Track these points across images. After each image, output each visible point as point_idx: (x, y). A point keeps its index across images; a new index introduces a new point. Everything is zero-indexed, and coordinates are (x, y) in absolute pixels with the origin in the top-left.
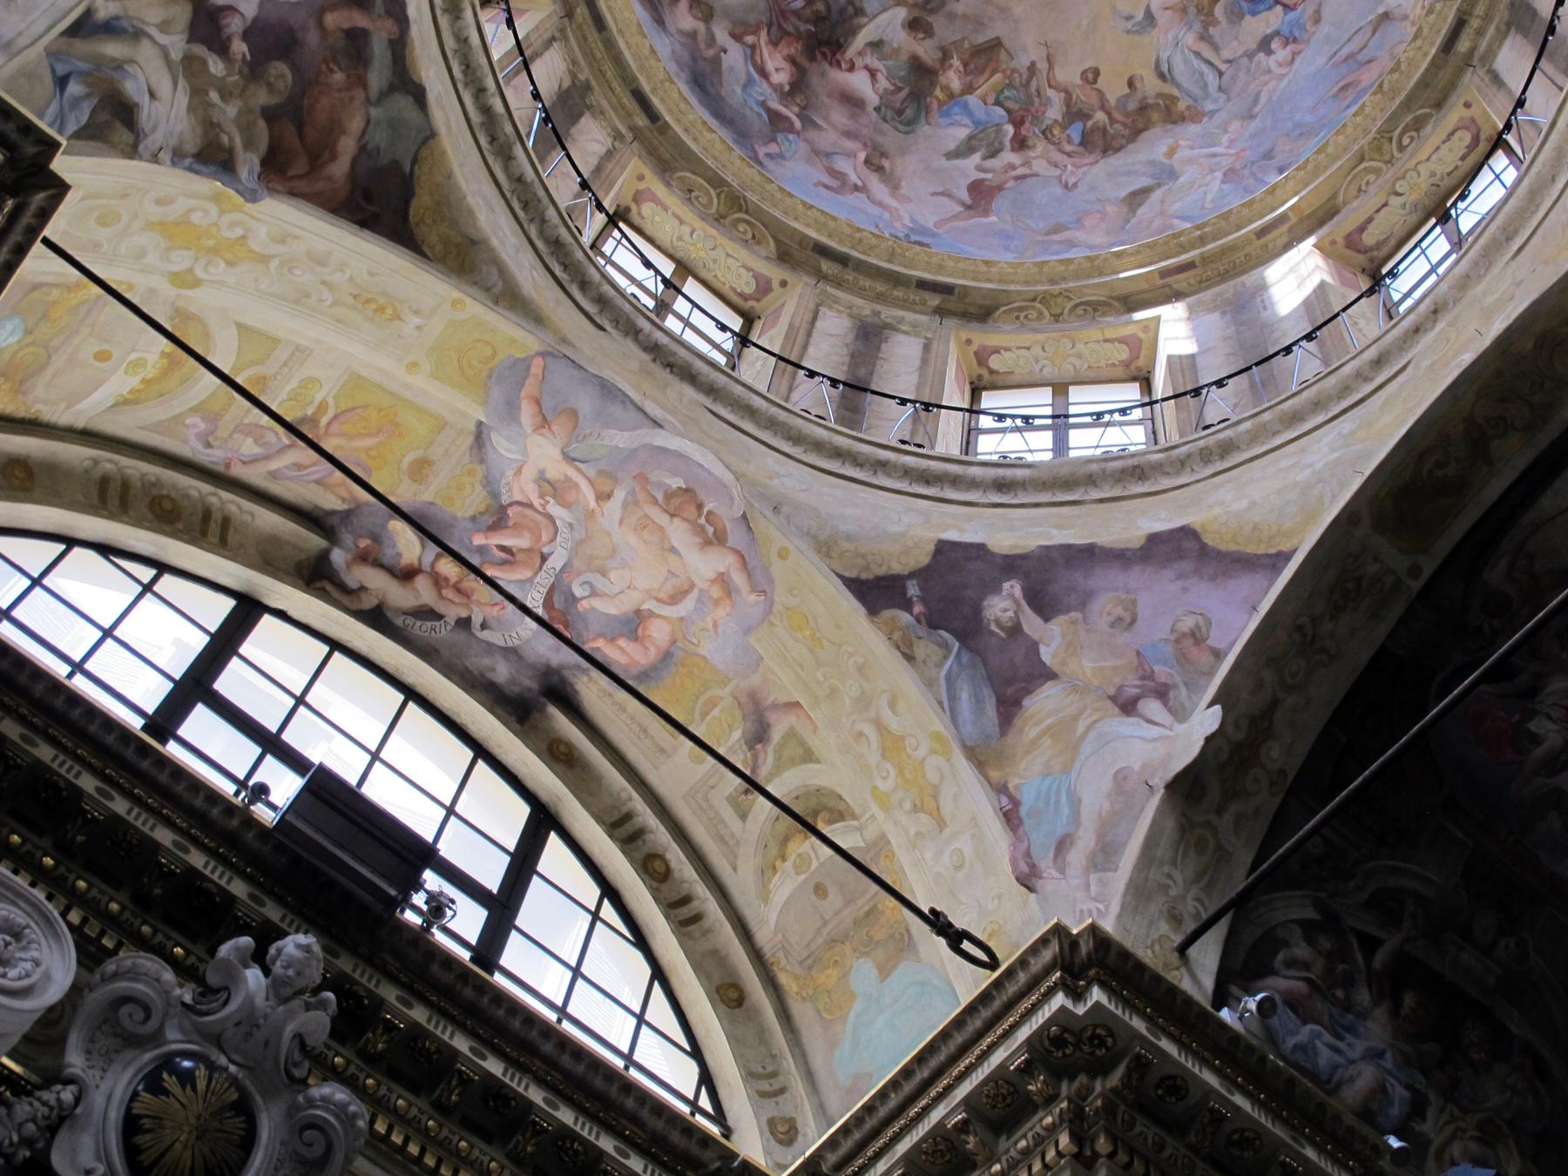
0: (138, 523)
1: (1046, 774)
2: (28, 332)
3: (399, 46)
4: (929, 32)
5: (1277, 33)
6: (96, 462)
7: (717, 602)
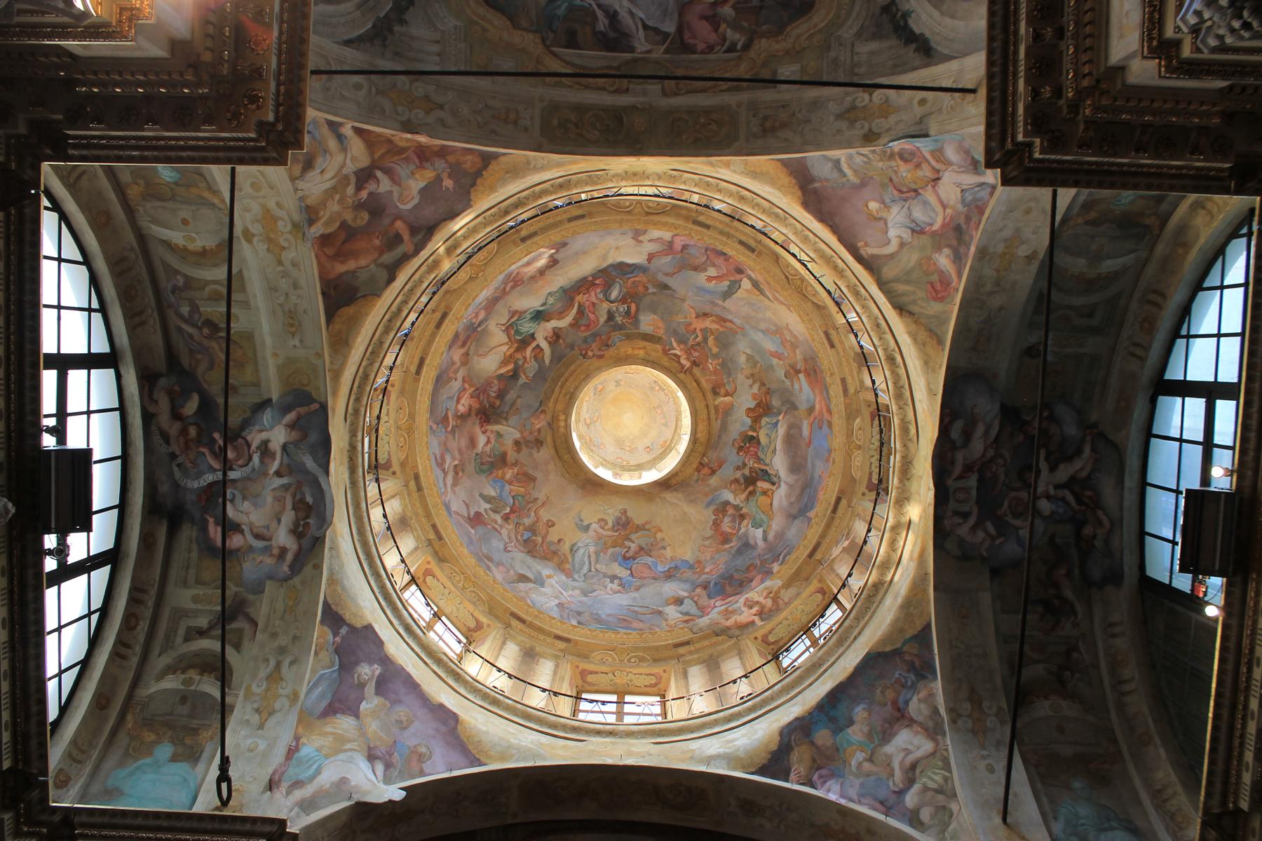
0: (117, 286)
1: (318, 750)
2: (176, 184)
3: (406, 258)
4: (519, 451)
5: (621, 579)
6: (132, 249)
7: (272, 555)
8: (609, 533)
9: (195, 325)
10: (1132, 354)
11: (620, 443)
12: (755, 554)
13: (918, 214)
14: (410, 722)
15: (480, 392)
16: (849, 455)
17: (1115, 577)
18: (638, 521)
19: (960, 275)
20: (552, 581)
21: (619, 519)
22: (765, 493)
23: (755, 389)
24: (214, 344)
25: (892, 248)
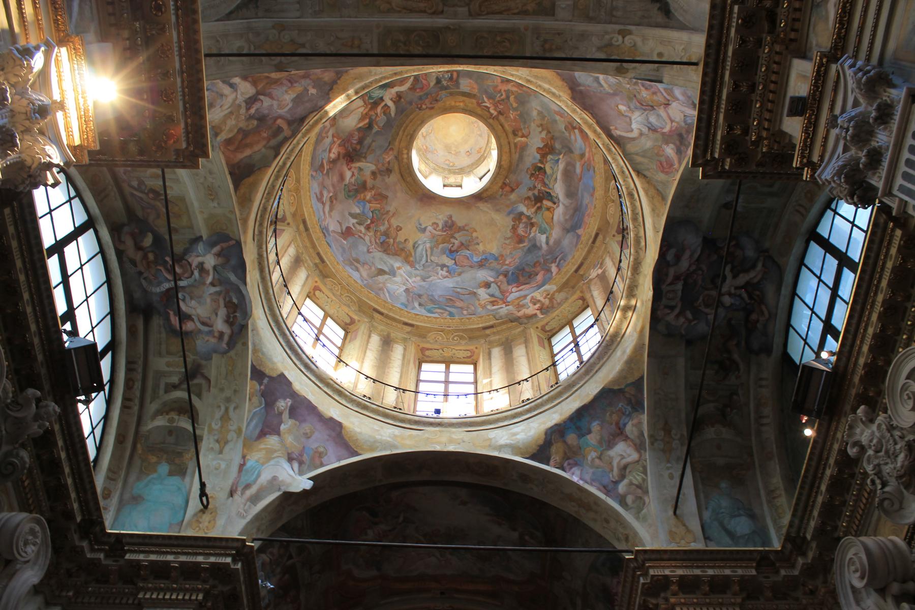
0: (85, 180)
1: (257, 461)
4: (375, 179)
5: (448, 267)
7: (214, 337)
8: (440, 233)
9: (142, 192)
10: (798, 211)
11: (448, 148)
12: (540, 254)
13: (653, 119)
14: (312, 433)
15: (345, 141)
16: (606, 205)
17: (767, 350)
18: (460, 223)
19: (680, 163)
20: (401, 271)
21: (446, 222)
22: (548, 209)
23: (544, 135)
24: (158, 204)
25: (635, 134)
